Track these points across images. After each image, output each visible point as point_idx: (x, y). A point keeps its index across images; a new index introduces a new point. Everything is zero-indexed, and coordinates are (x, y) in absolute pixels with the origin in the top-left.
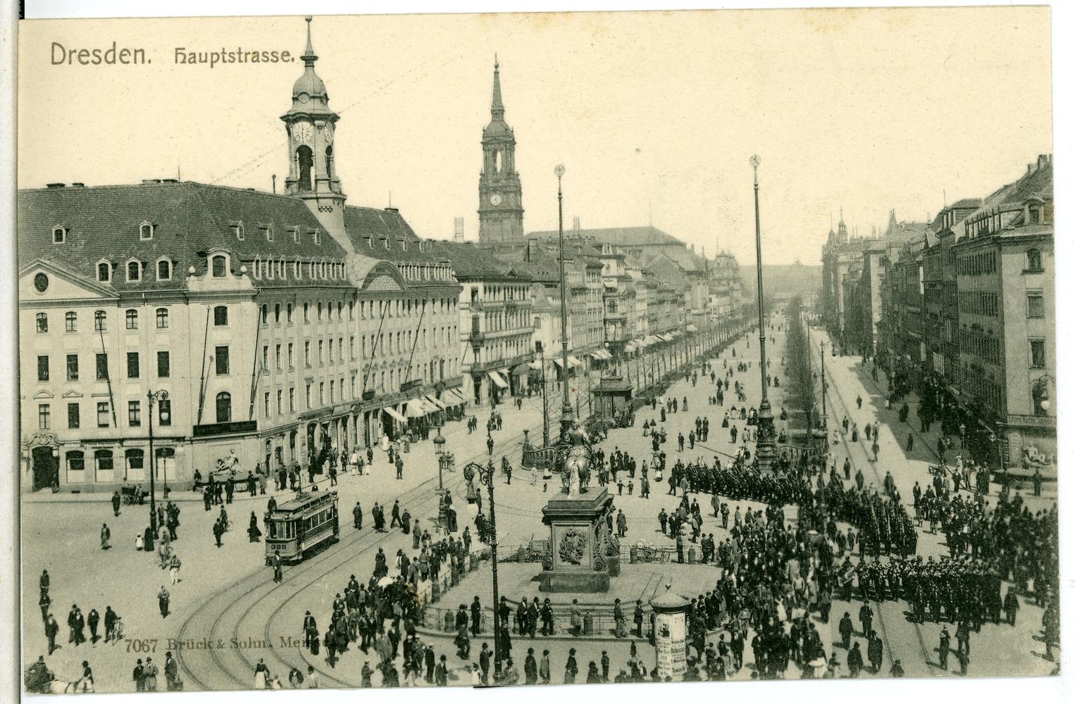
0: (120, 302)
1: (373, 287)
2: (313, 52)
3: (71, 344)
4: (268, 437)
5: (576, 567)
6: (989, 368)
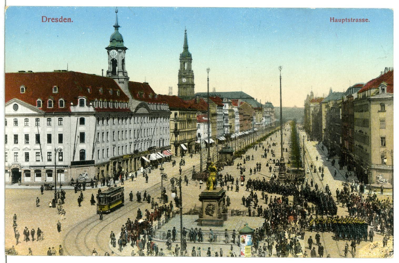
0: (44, 116)
1: (138, 112)
3: (27, 130)
4: (99, 166)
5: (211, 217)
6: (365, 146)
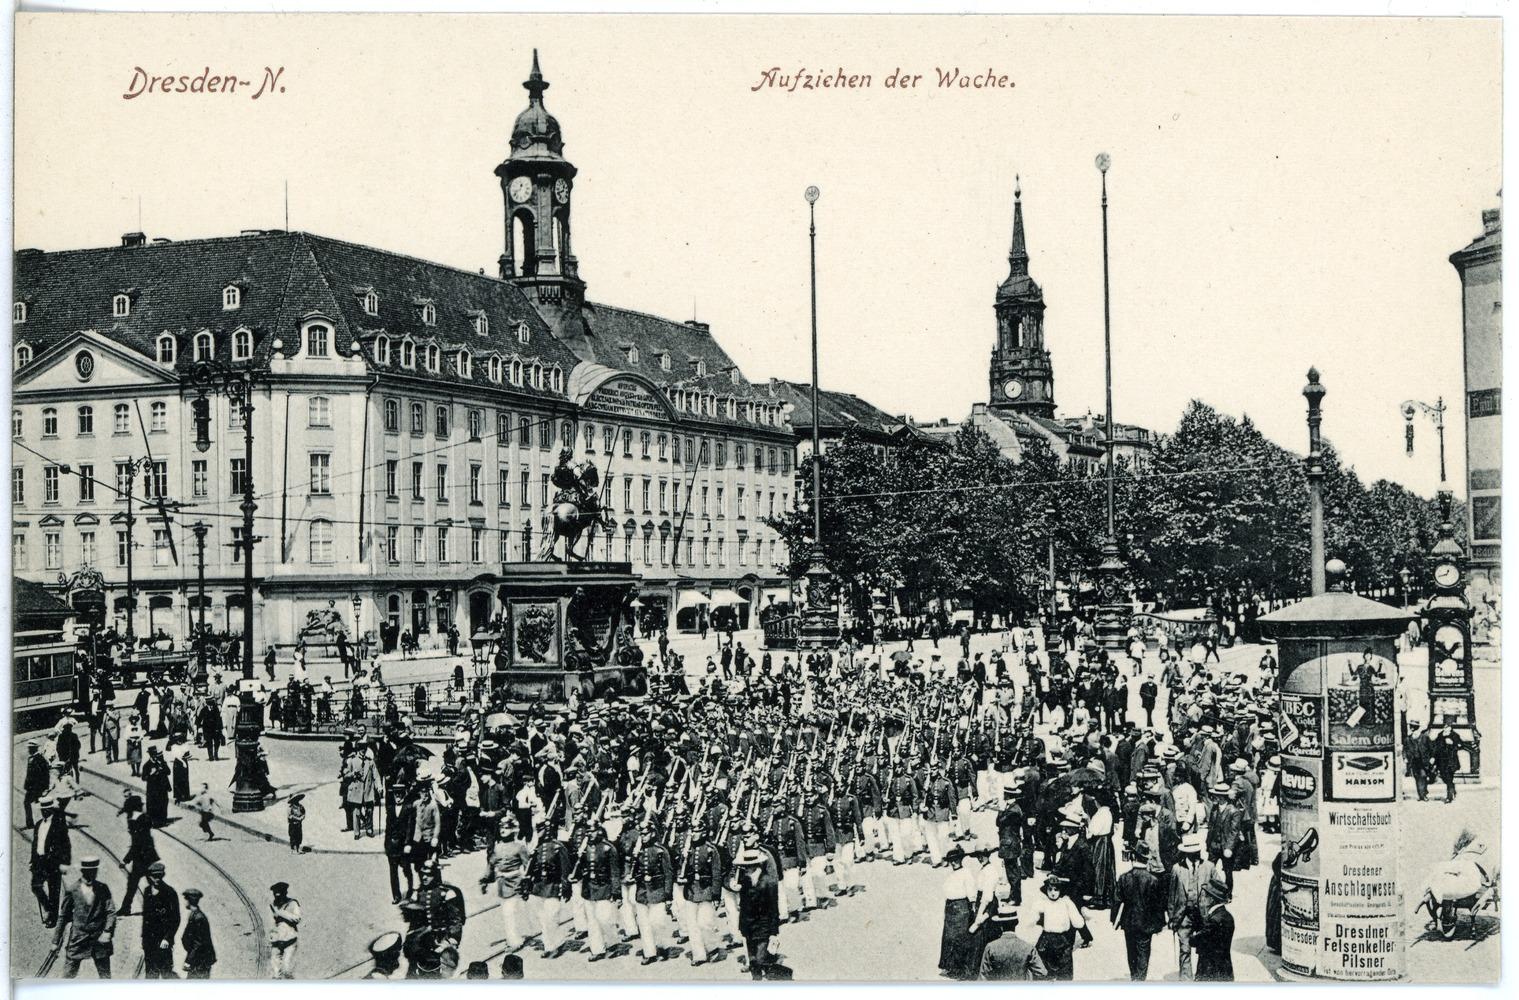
2: (540, 76)
